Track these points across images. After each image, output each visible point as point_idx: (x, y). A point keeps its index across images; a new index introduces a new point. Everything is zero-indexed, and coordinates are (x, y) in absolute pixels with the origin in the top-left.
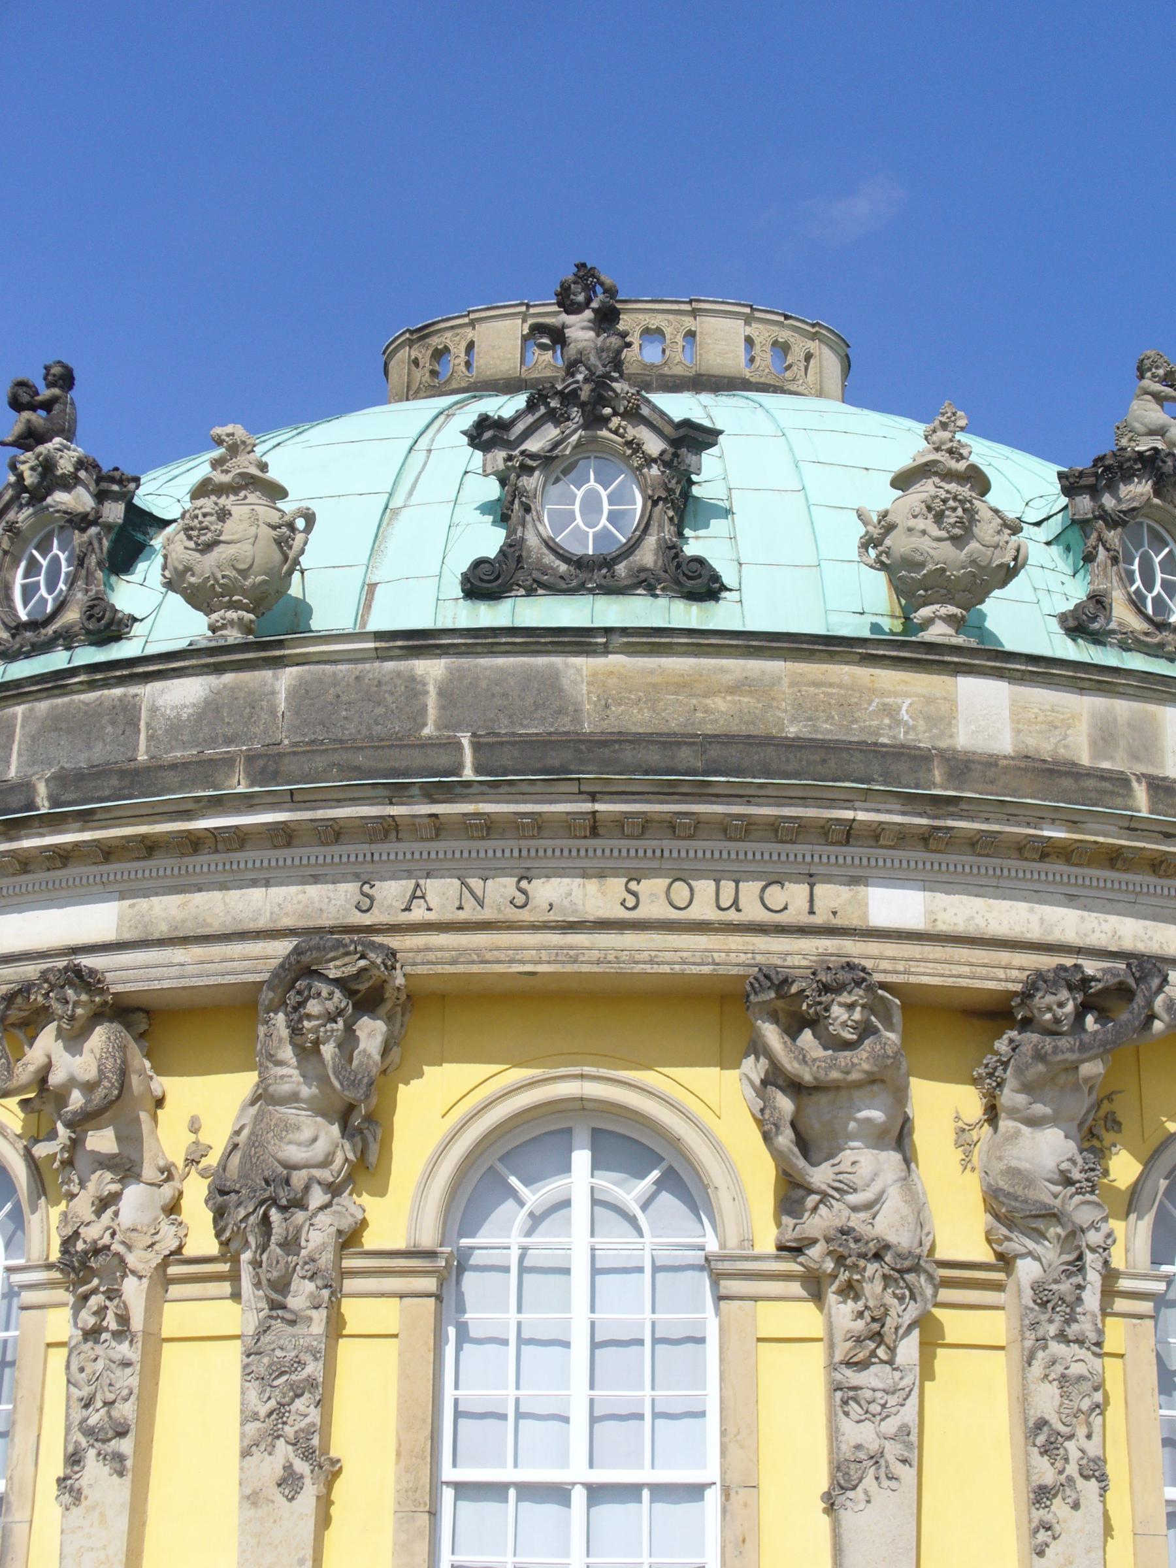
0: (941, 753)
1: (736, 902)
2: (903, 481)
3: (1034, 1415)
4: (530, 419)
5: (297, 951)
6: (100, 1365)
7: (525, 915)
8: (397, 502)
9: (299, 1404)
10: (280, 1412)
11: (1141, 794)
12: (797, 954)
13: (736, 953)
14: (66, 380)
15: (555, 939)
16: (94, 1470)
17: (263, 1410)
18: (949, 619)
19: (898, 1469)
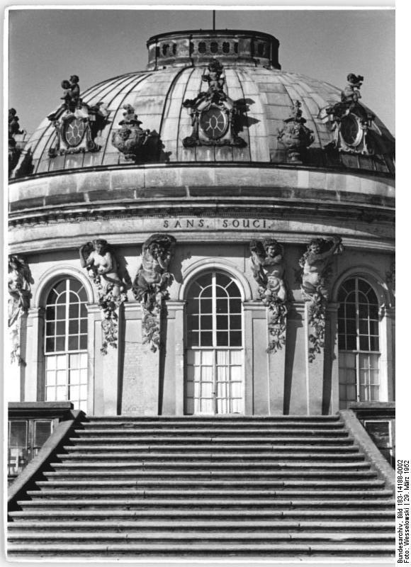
0: (294, 188)
1: (248, 226)
2: (287, 121)
3: (310, 333)
4: (199, 100)
5: (153, 237)
6: (109, 326)
7: (202, 229)
8: (165, 117)
9: (155, 333)
10: (151, 336)
11: (338, 197)
12: (261, 236)
13: (247, 236)
14: (76, 79)
15: (208, 234)
16: (110, 348)
17: (147, 335)
18: (296, 156)
19: (282, 345)
